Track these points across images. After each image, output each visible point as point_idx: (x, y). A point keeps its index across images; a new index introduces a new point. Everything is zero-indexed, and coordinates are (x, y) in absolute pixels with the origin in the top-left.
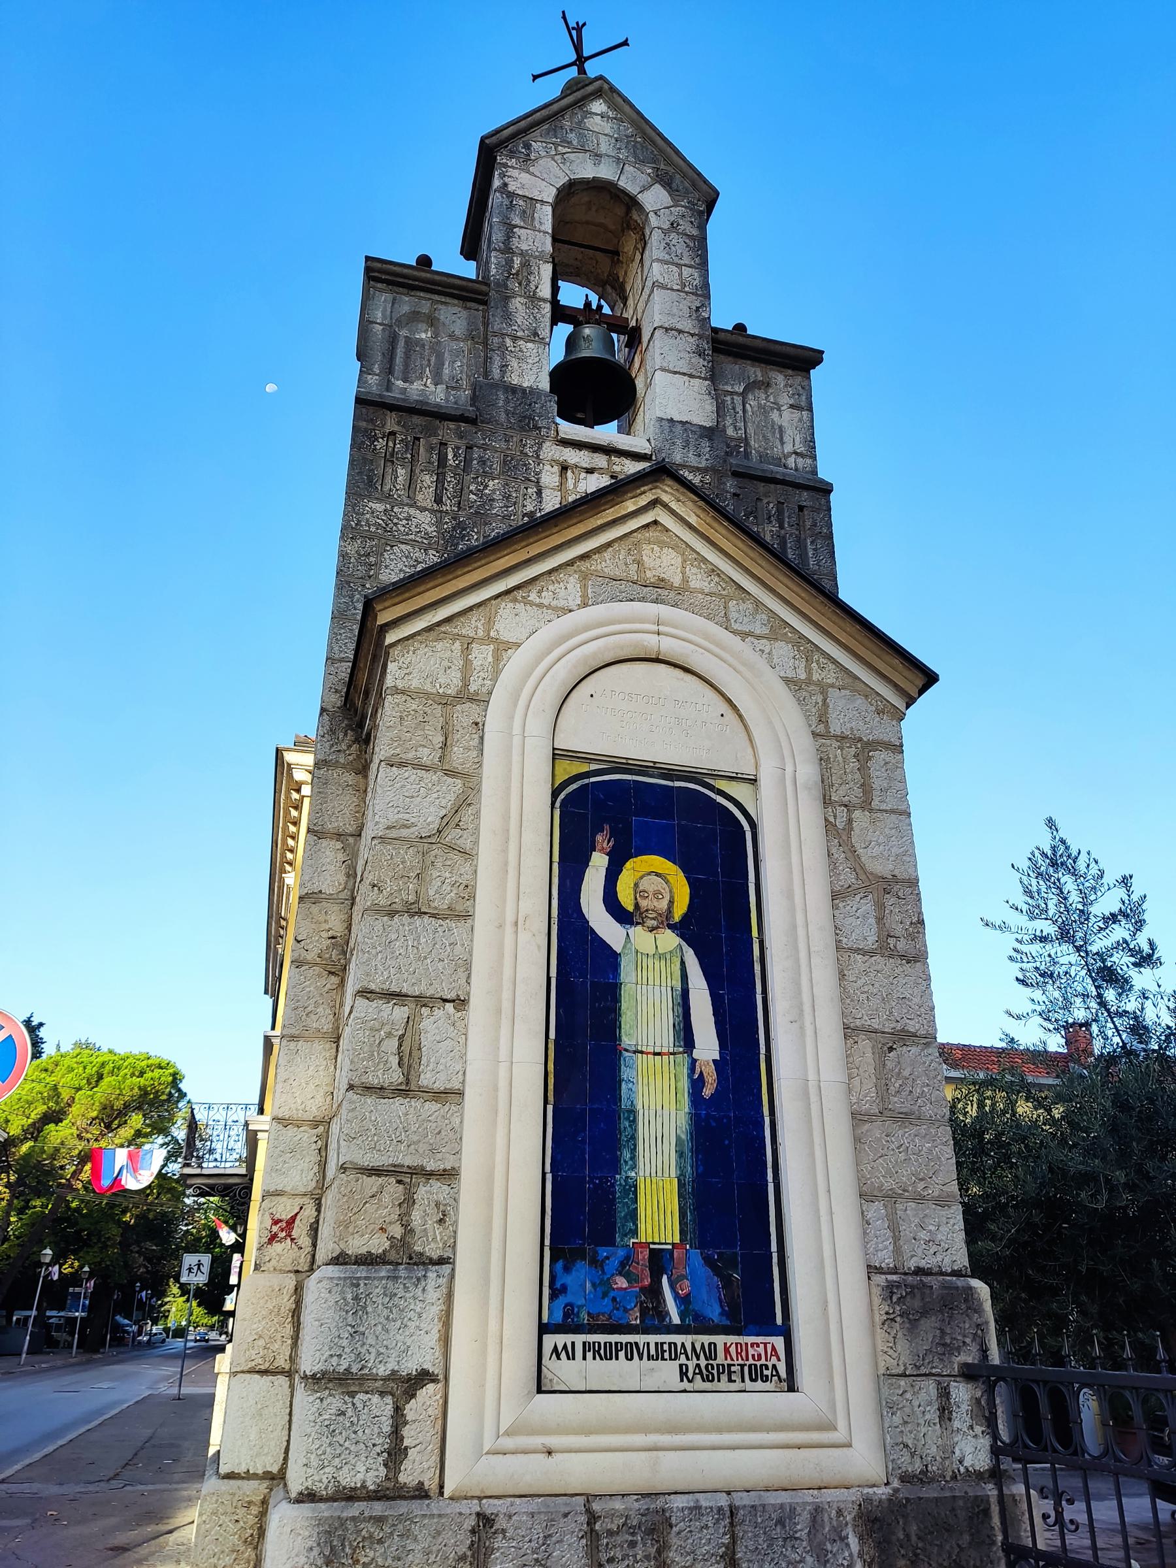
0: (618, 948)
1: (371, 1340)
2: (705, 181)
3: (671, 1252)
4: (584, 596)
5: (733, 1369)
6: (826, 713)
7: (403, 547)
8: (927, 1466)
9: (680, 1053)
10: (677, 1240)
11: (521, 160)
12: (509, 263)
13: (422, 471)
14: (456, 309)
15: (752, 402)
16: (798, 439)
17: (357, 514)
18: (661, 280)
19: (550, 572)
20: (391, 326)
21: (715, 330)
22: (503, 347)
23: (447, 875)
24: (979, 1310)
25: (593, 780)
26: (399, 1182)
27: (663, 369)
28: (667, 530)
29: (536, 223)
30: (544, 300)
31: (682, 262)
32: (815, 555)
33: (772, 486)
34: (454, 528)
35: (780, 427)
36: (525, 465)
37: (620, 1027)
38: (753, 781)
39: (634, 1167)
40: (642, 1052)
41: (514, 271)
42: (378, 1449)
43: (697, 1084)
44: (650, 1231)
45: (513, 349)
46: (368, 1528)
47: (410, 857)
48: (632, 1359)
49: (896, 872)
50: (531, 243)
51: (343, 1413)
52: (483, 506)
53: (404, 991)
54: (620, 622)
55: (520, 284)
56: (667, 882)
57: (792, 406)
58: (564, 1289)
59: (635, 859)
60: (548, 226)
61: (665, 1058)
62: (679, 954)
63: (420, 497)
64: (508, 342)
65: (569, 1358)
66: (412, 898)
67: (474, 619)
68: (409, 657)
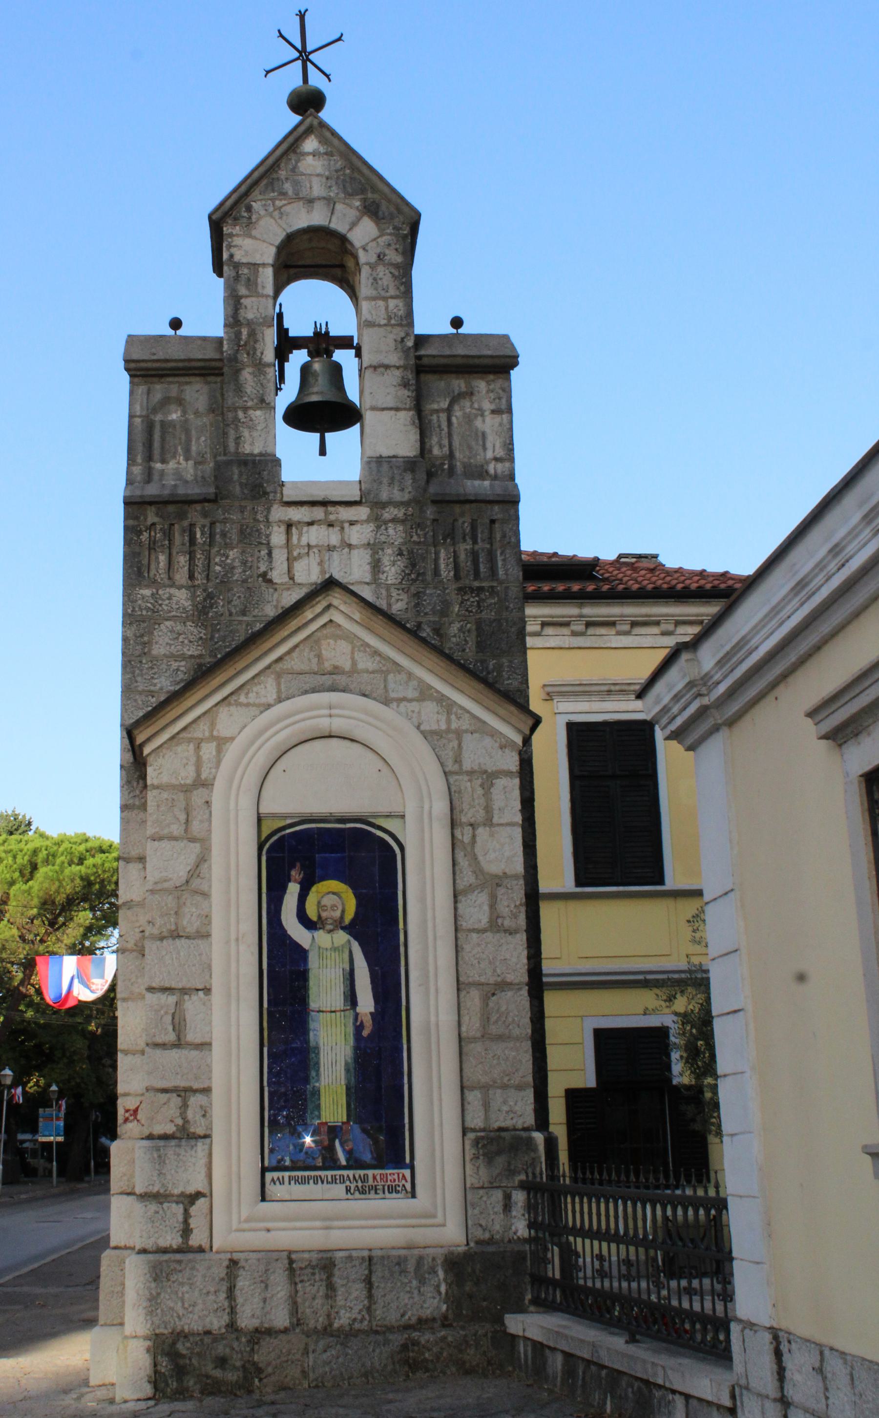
0: (306, 944)
1: (169, 1177)
2: (407, 204)
3: (341, 1127)
4: (279, 691)
6: (460, 754)
7: (168, 623)
10: (345, 1120)
11: (244, 225)
12: (238, 335)
13: (178, 553)
14: (198, 386)
15: (457, 413)
16: (498, 445)
17: (132, 602)
18: (370, 319)
19: (253, 678)
20: (147, 416)
22: (236, 419)
23: (194, 910)
24: (535, 1150)
25: (288, 831)
26: (179, 1096)
27: (373, 408)
28: (340, 626)
29: (260, 290)
31: (388, 294)
32: (504, 565)
33: (467, 506)
34: (205, 600)
35: (484, 435)
36: (257, 530)
39: (318, 1080)
40: (323, 1012)
41: (242, 343)
42: (177, 1229)
43: (359, 1029)
45: (244, 420)
46: (173, 1266)
47: (170, 901)
49: (507, 871)
50: (255, 311)
51: (157, 1212)
52: (225, 575)
53: (173, 986)
54: (302, 712)
55: (248, 354)
56: (340, 897)
57: (493, 412)
61: (338, 1014)
63: (177, 577)
64: (241, 414)
66: (173, 927)
67: (202, 724)
68: (160, 761)
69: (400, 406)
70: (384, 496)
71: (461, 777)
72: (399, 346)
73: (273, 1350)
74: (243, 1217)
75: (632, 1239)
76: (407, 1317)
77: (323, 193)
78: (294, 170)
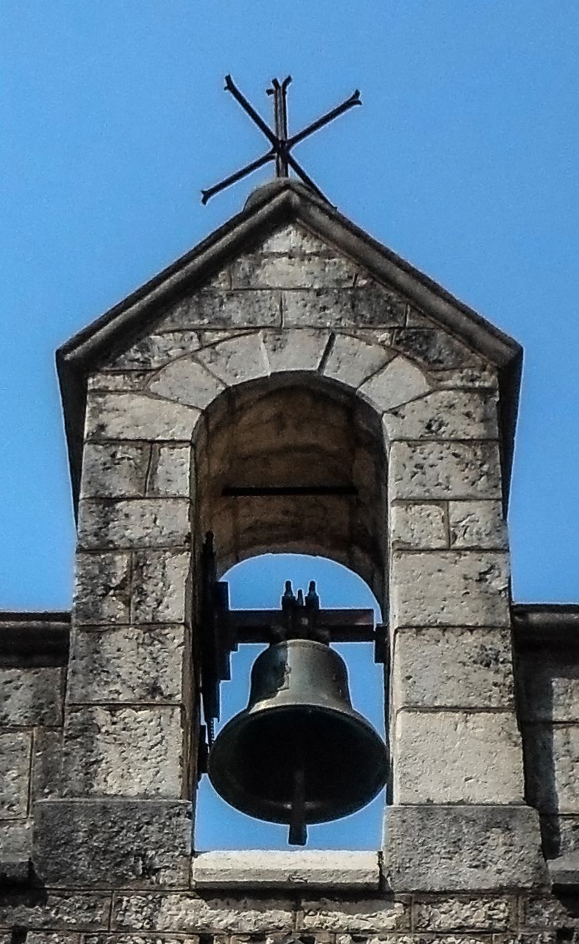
21: (519, 611)
30: (173, 625)
31: (449, 494)
41: (115, 582)
60: (182, 485)
64: (102, 716)
69: (476, 702)
70: (436, 878)
72: (475, 590)
77: (310, 318)
78: (247, 287)
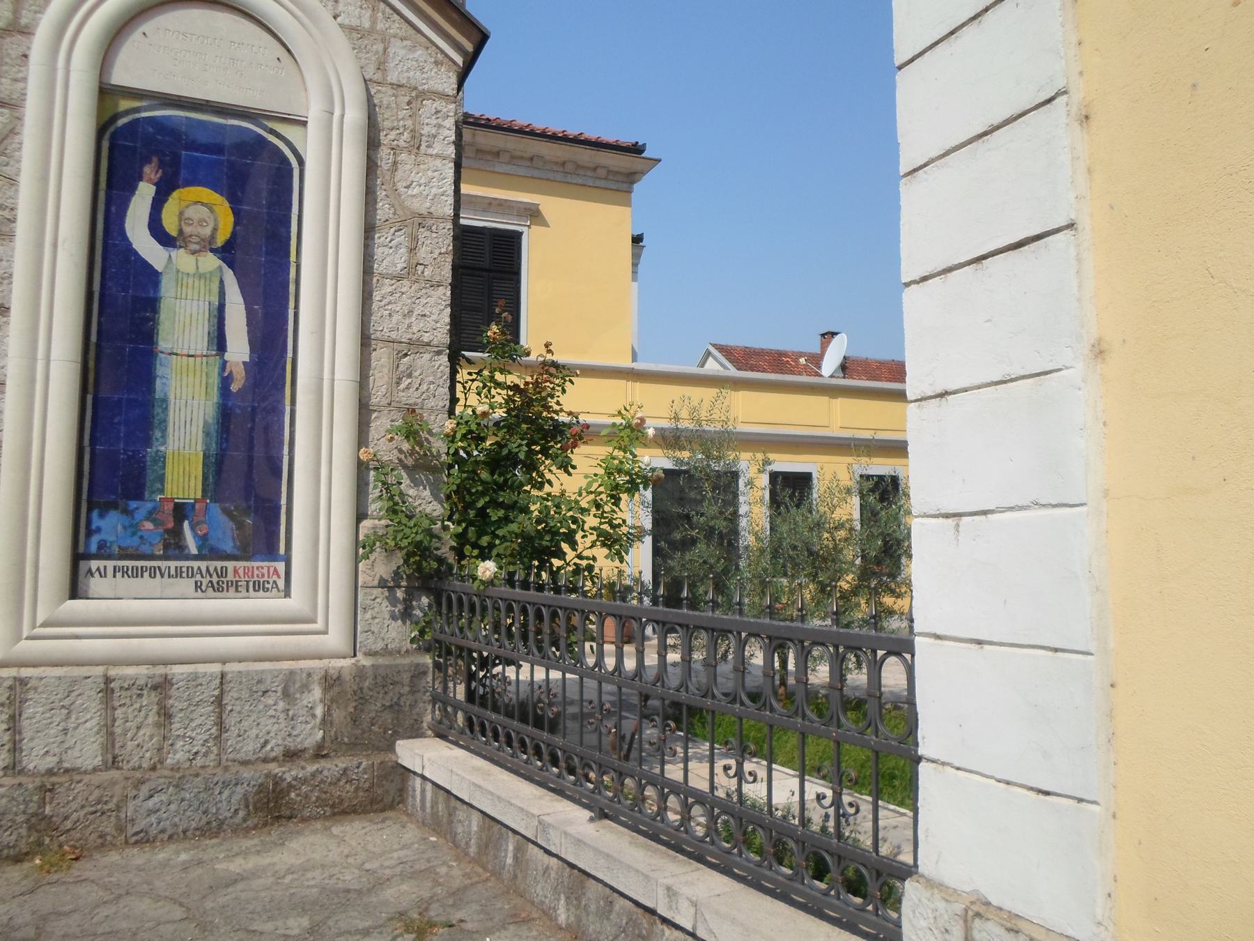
0: (159, 267)
3: (193, 505)
5: (239, 584)
8: (387, 645)
9: (212, 356)
10: (199, 496)
37: (157, 334)
38: (304, 124)
39: (164, 443)
40: (177, 354)
43: (226, 381)
44: (175, 490)
48: (155, 577)
49: (432, 210)
58: (99, 530)
59: (181, 190)
61: (198, 359)
62: (219, 275)
65: (101, 576)
71: (383, 89)
73: (74, 799)
74: (41, 618)
75: (612, 673)
76: (268, 747)
